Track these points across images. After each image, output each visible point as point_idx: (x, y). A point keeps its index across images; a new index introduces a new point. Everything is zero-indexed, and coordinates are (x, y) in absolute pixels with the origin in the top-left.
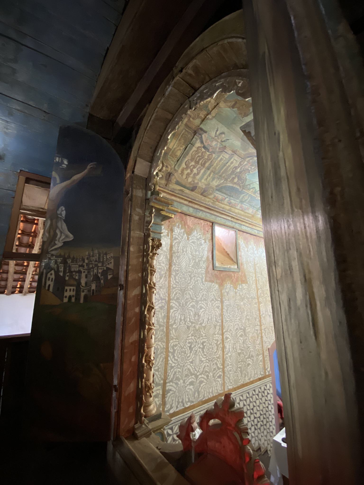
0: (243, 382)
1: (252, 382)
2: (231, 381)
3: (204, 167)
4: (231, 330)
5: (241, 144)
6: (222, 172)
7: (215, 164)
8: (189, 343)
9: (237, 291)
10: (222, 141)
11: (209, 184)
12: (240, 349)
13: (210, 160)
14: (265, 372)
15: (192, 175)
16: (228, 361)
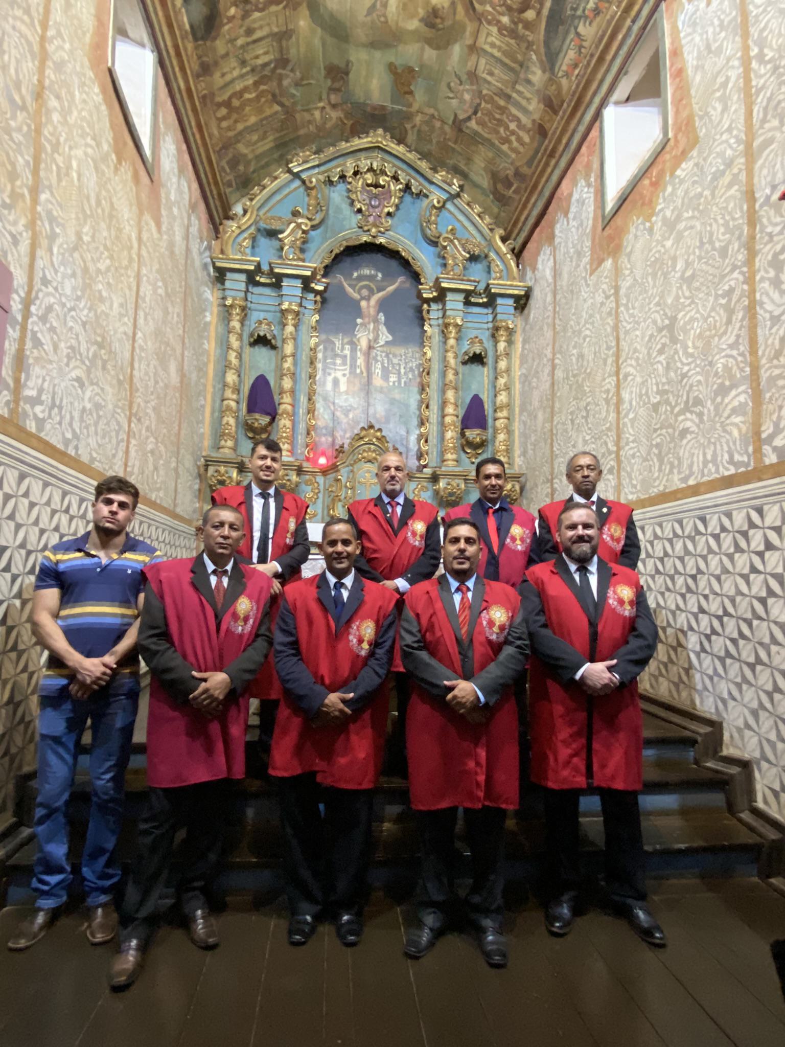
0: (665, 486)
1: (695, 490)
2: (634, 482)
3: (506, 108)
4: (635, 350)
5: (455, 41)
6: (513, 65)
7: (499, 85)
8: (572, 413)
9: (654, 219)
10: (461, 83)
11: (538, 91)
12: (658, 392)
13: (492, 98)
14: (758, 451)
15: (521, 133)
16: (629, 433)
